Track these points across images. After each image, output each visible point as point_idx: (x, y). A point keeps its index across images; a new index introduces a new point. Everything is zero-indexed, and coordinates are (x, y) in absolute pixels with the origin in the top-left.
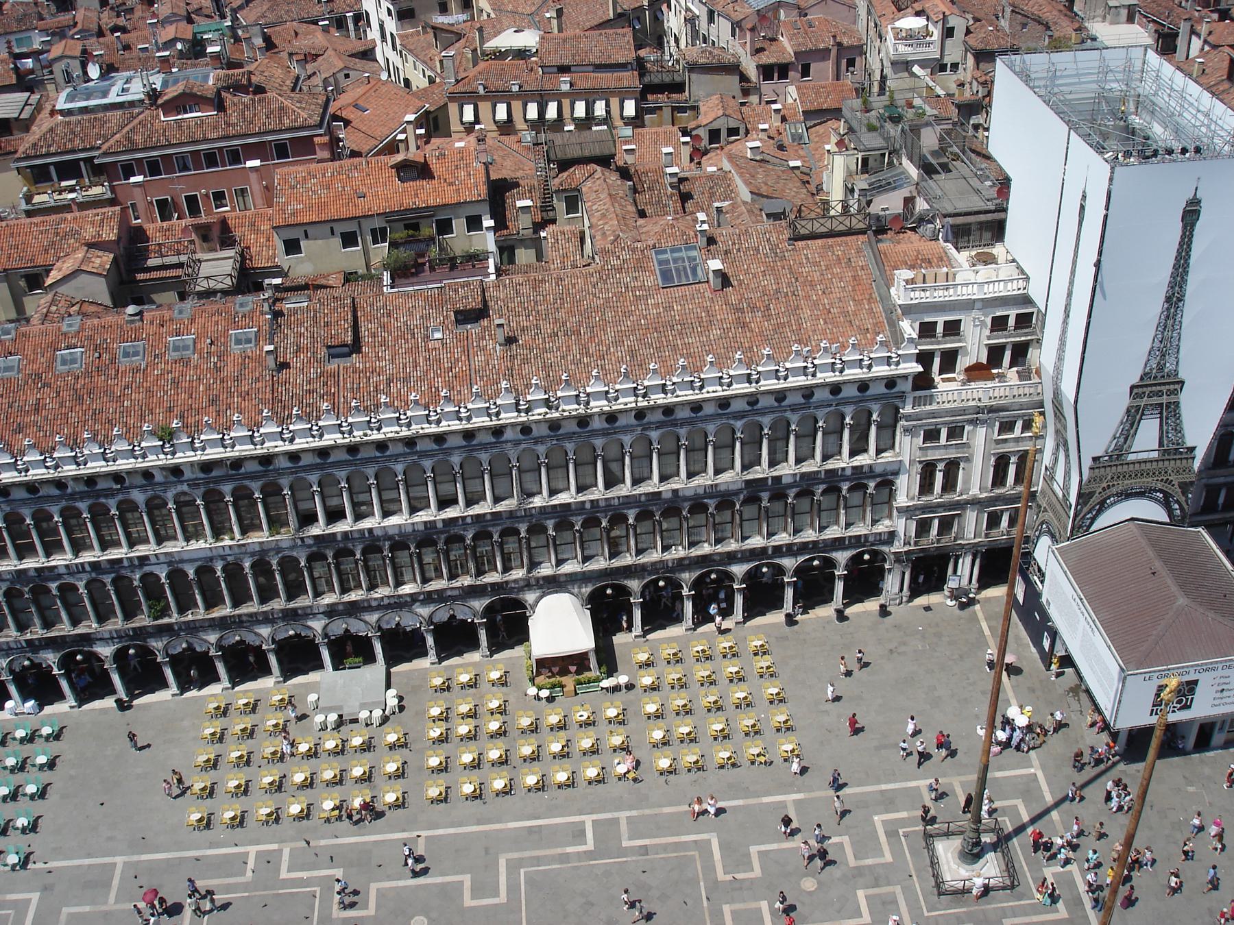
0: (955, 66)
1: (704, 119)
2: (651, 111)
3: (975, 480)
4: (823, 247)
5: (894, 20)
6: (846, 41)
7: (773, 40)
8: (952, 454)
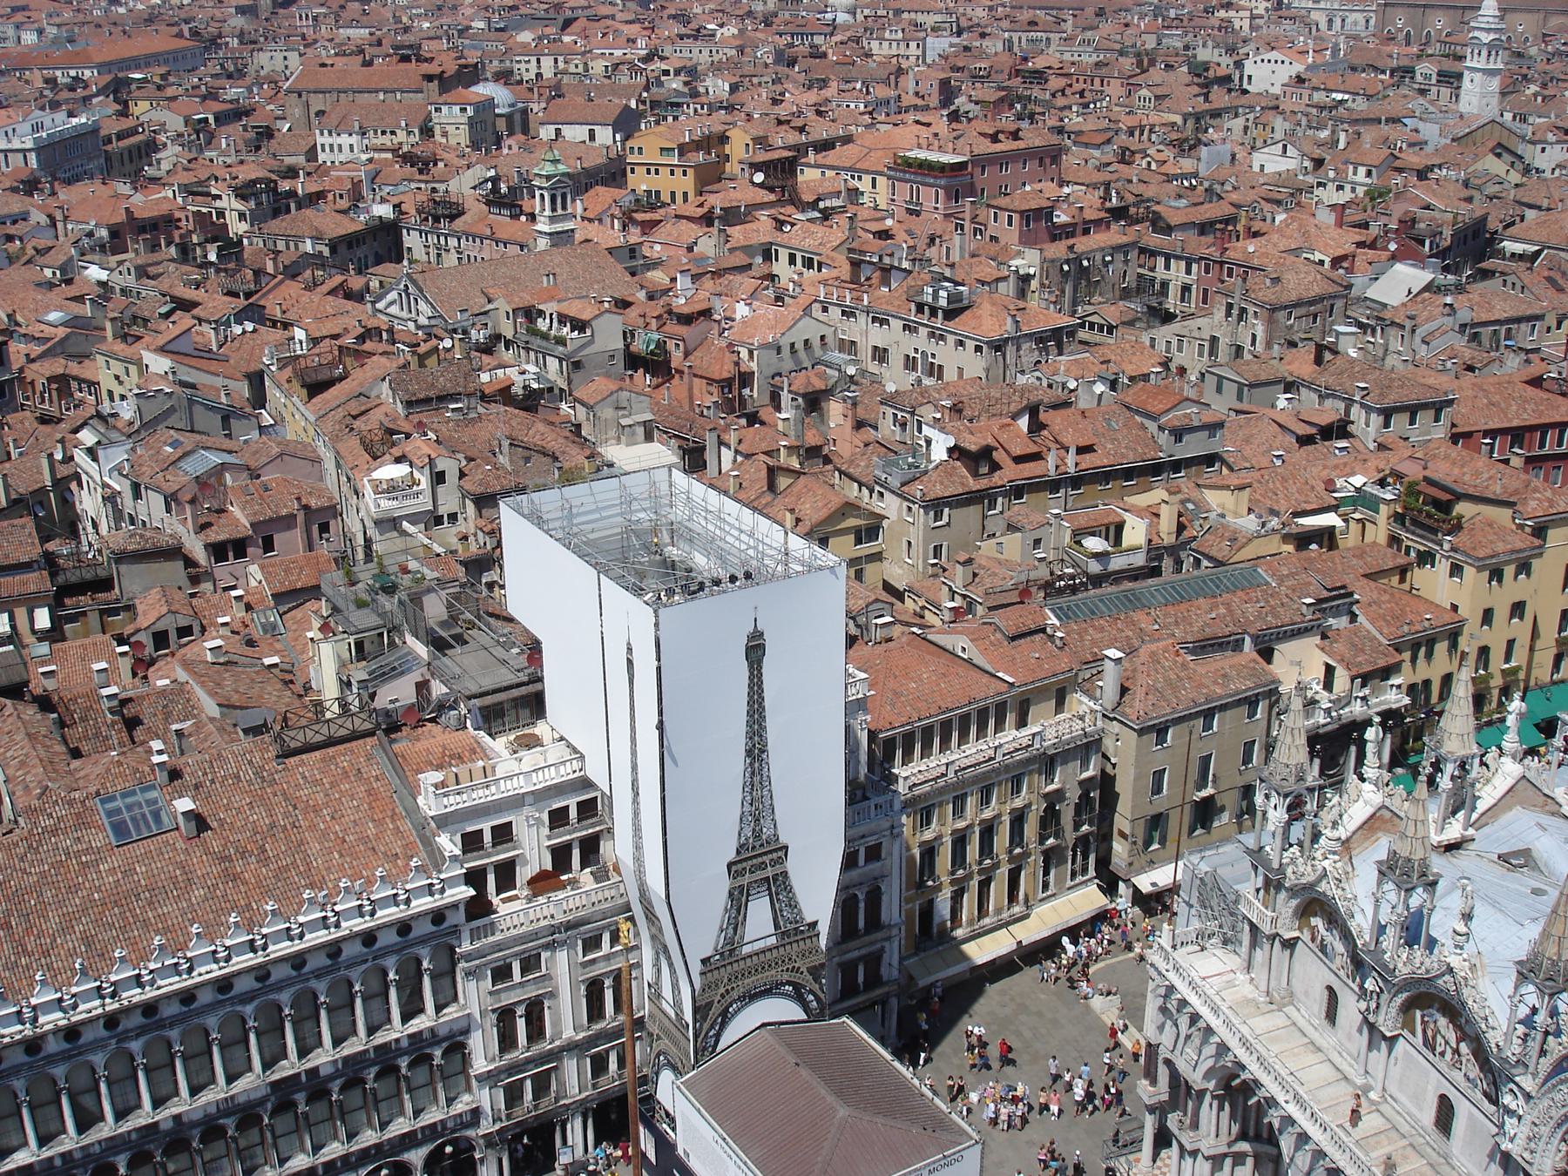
0: (453, 517)
1: (143, 622)
2: (72, 619)
3: (566, 1019)
4: (323, 760)
5: (370, 471)
6: (313, 503)
7: (221, 511)
8: (531, 992)
